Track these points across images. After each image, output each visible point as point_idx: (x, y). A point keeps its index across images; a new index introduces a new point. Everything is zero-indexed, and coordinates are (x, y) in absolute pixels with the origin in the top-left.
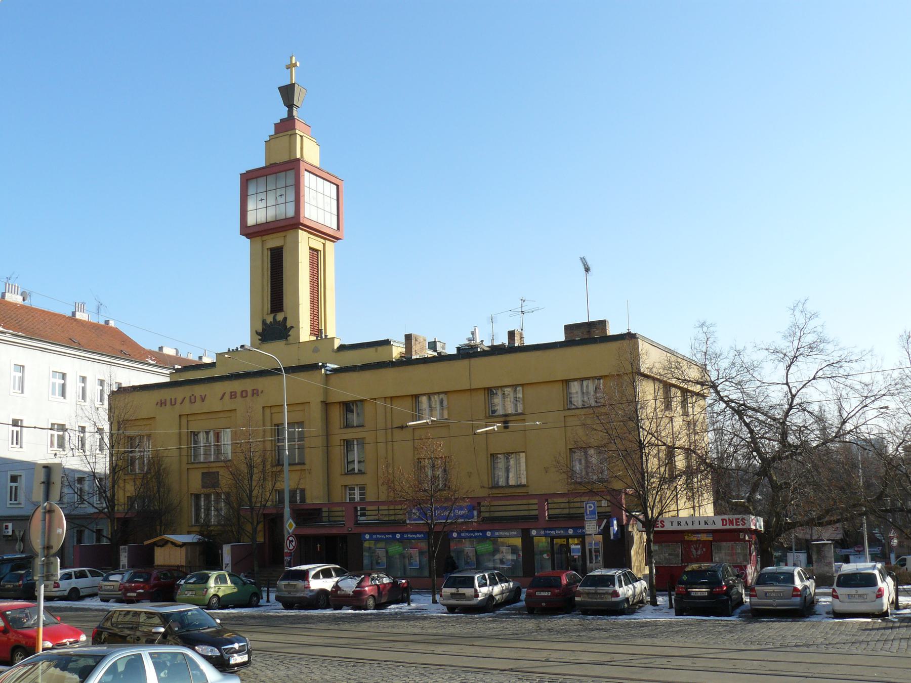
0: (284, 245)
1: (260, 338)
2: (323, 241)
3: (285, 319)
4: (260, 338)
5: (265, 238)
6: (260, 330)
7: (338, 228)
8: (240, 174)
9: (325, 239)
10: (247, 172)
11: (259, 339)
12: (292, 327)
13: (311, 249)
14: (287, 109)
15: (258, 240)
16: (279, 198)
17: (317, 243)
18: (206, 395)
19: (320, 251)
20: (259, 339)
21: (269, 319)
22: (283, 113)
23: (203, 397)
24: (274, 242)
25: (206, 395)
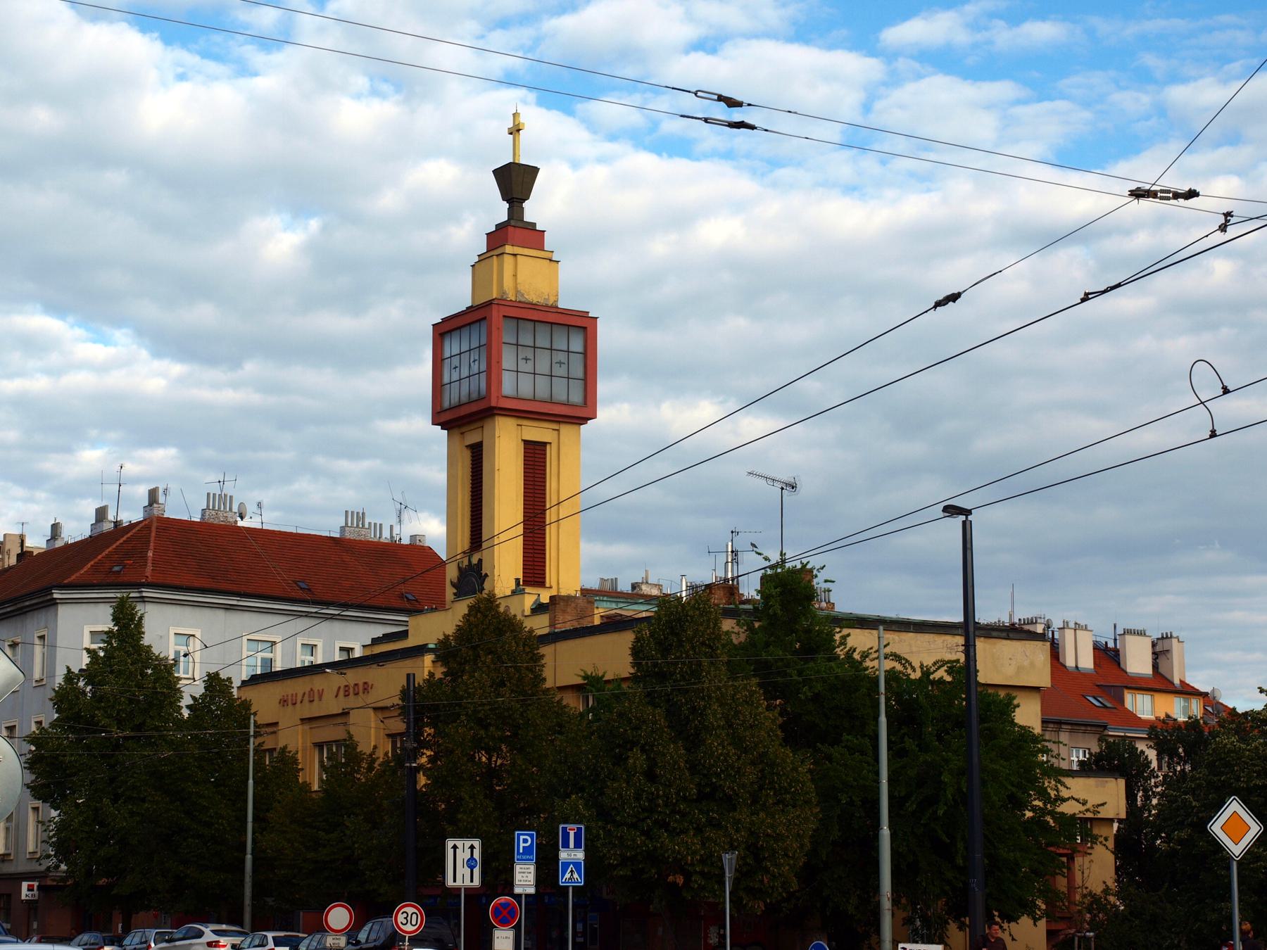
0: (482, 441)
1: (455, 591)
2: (555, 426)
3: (480, 561)
4: (455, 591)
5: (463, 429)
6: (456, 581)
7: (585, 403)
8: (433, 325)
9: (559, 422)
10: (445, 320)
11: (455, 594)
12: (486, 575)
13: (526, 442)
14: (507, 205)
15: (456, 432)
16: (472, 364)
17: (537, 432)
18: (323, 690)
19: (550, 443)
20: (455, 594)
21: (466, 562)
22: (501, 211)
23: (321, 691)
24: (472, 438)
25: (323, 690)
